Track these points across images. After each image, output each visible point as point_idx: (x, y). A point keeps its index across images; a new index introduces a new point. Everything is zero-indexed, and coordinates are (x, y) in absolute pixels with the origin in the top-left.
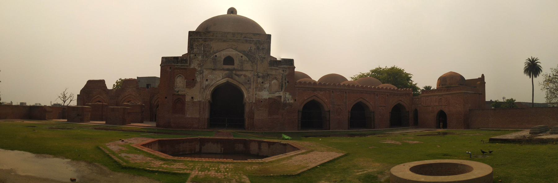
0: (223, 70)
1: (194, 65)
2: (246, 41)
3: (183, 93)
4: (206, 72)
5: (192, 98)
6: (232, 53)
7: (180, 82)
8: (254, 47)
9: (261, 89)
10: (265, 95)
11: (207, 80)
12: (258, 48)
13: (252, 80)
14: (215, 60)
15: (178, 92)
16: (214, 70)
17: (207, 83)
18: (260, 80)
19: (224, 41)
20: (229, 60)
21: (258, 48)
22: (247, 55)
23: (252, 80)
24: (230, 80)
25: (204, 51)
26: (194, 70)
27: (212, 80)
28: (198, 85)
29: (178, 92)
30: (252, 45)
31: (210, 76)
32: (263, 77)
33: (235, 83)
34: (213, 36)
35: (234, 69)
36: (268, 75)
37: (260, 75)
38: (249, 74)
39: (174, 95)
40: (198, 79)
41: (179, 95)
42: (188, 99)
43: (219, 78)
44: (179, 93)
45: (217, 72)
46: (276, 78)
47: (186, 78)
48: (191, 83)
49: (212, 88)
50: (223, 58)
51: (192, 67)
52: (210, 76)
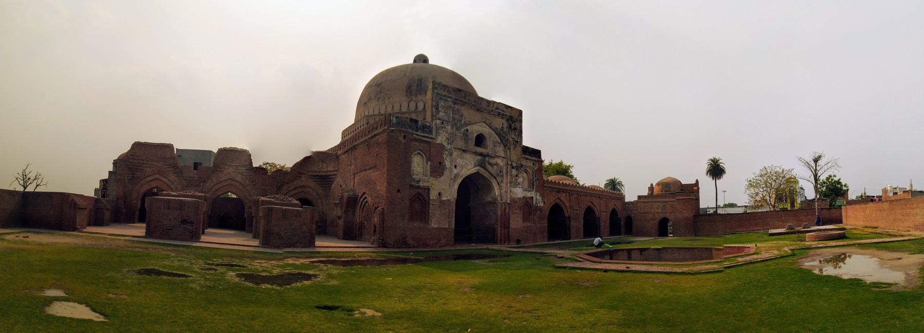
0: (476, 153)
1: (441, 139)
2: (499, 114)
3: (426, 184)
4: (455, 154)
5: (439, 194)
6: (485, 130)
7: (418, 165)
8: (506, 125)
9: (516, 184)
10: (519, 193)
11: (456, 167)
12: (510, 126)
13: (504, 171)
14: (466, 134)
15: (418, 182)
16: (464, 151)
17: (455, 171)
18: (514, 172)
19: (478, 110)
20: (480, 140)
21: (510, 126)
22: (499, 135)
23: (504, 171)
24: (482, 171)
25: (454, 119)
26: (442, 146)
27: (462, 167)
28: (447, 173)
29: (418, 182)
30: (504, 121)
31: (459, 161)
32: (517, 168)
33: (486, 175)
34: (465, 97)
35: (488, 155)
36: (522, 166)
37: (514, 165)
38: (501, 162)
39: (411, 186)
40: (447, 164)
41: (419, 187)
42: (433, 195)
43: (467, 166)
44: (421, 184)
45: (467, 156)
46: (526, 172)
47: (428, 159)
48: (438, 170)
49: (459, 181)
50: (475, 135)
51: (438, 141)
52: (459, 161)
